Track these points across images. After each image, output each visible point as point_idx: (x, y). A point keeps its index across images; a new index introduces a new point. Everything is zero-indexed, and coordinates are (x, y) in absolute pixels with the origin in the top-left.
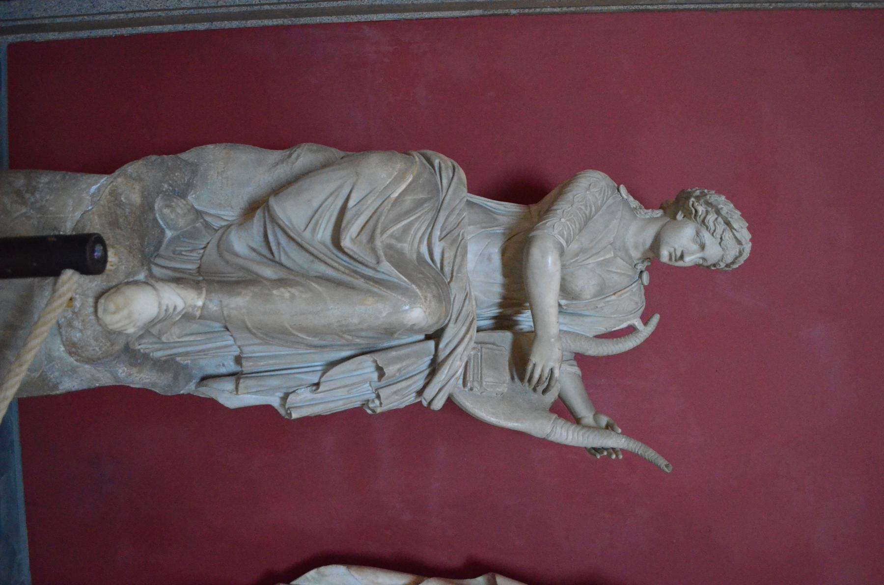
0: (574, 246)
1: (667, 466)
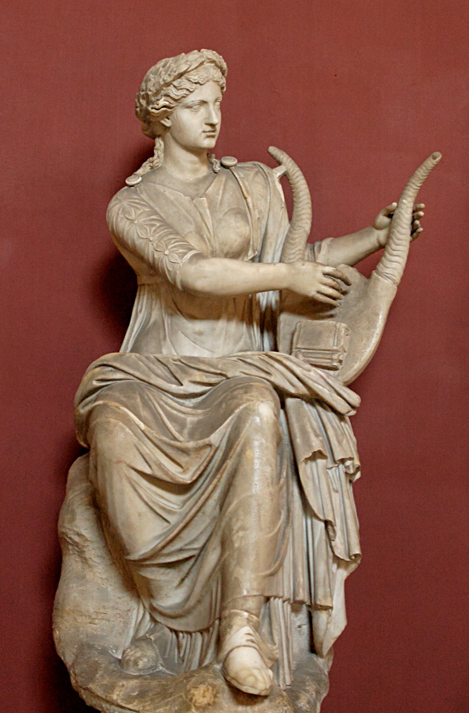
0: (193, 241)
1: (434, 158)
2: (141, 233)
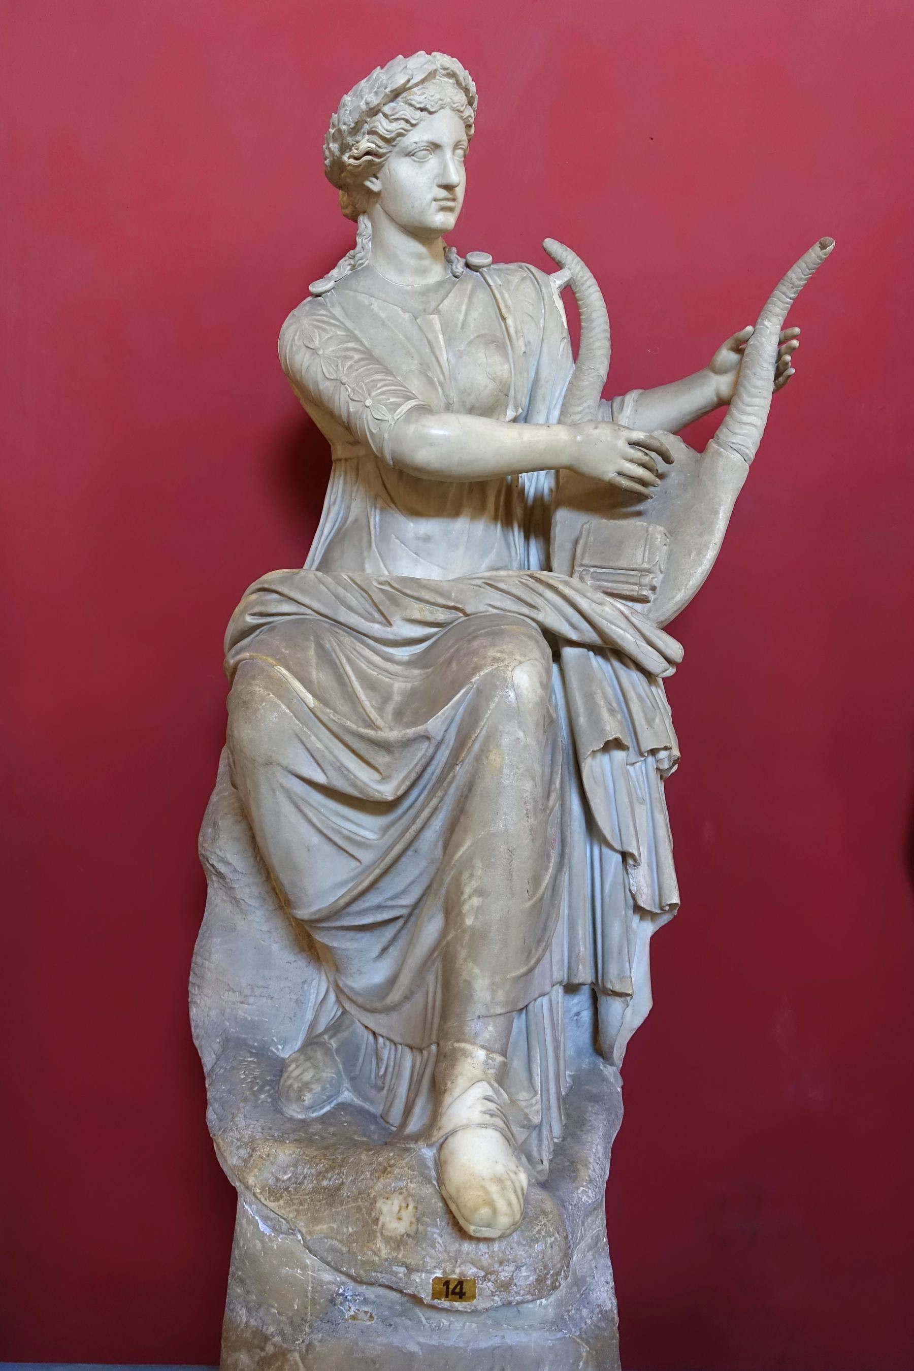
0: (415, 385)
1: (823, 247)
2: (329, 372)
